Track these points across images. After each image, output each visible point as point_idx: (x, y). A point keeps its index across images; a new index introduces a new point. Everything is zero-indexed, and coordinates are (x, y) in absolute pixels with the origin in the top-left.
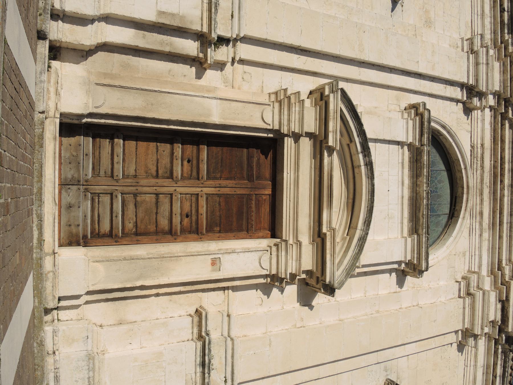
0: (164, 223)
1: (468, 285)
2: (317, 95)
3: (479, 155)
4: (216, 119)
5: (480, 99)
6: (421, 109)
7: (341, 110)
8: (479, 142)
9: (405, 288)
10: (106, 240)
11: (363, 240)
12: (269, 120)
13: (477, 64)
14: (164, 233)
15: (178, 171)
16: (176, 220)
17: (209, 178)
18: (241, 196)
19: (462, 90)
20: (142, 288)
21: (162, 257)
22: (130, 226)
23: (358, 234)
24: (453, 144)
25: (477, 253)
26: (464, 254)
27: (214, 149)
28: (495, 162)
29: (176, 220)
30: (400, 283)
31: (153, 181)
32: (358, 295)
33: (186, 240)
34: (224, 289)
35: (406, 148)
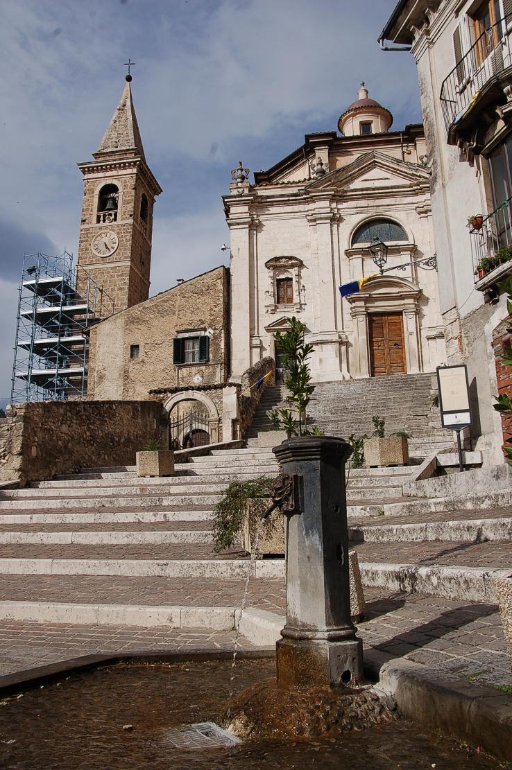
20: (419, 356)
34: (420, 330)
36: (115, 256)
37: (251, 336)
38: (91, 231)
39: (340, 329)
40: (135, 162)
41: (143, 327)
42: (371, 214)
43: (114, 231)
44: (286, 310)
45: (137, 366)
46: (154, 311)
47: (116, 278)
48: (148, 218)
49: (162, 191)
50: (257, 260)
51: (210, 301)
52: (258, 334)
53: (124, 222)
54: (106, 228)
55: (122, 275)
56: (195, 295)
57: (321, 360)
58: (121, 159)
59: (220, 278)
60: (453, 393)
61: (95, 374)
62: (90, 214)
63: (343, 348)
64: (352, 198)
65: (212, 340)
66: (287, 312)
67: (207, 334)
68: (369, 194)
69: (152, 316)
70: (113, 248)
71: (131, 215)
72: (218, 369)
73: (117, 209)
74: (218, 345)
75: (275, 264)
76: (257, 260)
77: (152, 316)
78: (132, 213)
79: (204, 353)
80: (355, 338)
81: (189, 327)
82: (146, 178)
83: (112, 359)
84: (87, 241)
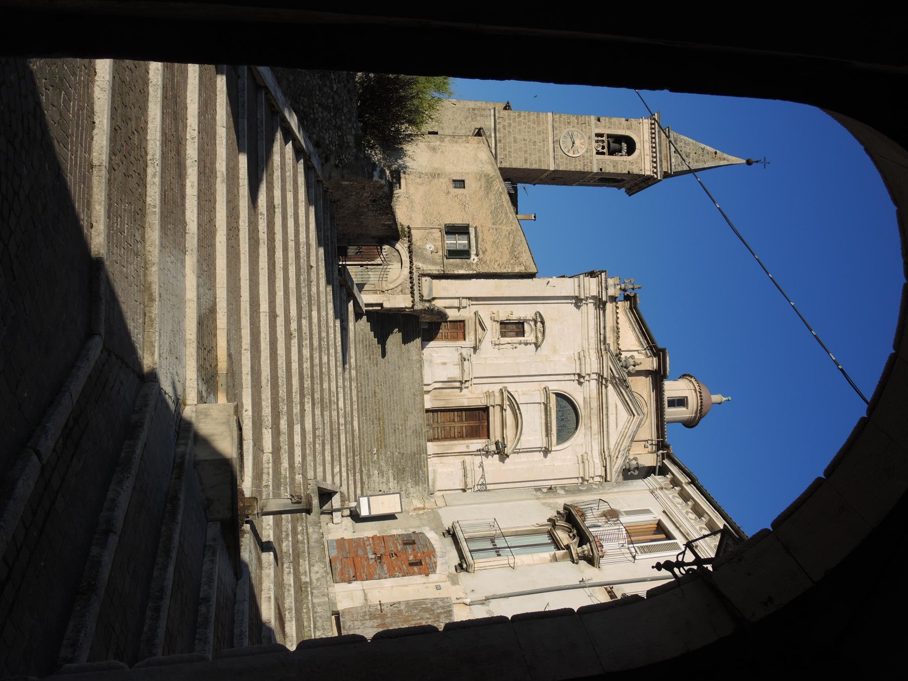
0: (452, 435)
1: (583, 459)
2: (501, 391)
3: (589, 401)
4: (466, 405)
5: (584, 379)
6: (547, 389)
7: (508, 396)
8: (588, 396)
9: (548, 458)
10: (437, 440)
11: (519, 439)
12: (483, 402)
13: (581, 364)
14: (453, 438)
15: (456, 420)
16: (456, 434)
17: (466, 421)
18: (477, 426)
19: (574, 375)
21: (452, 445)
22: (443, 436)
23: (518, 437)
24: (572, 399)
25: (590, 445)
26: (582, 445)
27: (467, 412)
28: (599, 403)
29: (456, 434)
30: (545, 456)
31: (449, 423)
32: (525, 460)
33: (459, 440)
34: (472, 455)
35: (542, 404)
36: (560, 153)
37: (469, 298)
38: (588, 127)
39: (475, 381)
40: (656, 173)
41: (482, 193)
42: (582, 412)
43: (587, 152)
44: (494, 331)
45: (444, 187)
46: (497, 204)
48: (600, 184)
49: (630, 195)
50: (543, 303)
51: (505, 260)
52: (472, 305)
53: (595, 162)
54: (590, 144)
55: (540, 161)
56: (511, 245)
57: (444, 364)
58: (661, 161)
59: (526, 270)
60: (383, 503)
61: (438, 143)
62: (605, 126)
63: (458, 384)
64: (600, 393)
65: (467, 262)
66: (493, 329)
67: (473, 257)
68: (602, 408)
69: (493, 201)
70: (569, 152)
71: (601, 169)
72: (438, 268)
73: (609, 155)
74: (462, 268)
75: (539, 320)
76: (543, 303)
77: (493, 201)
78: (603, 170)
79: (453, 253)
80: (466, 395)
81: (480, 239)
82: (641, 182)
83: (452, 161)
84: (578, 123)
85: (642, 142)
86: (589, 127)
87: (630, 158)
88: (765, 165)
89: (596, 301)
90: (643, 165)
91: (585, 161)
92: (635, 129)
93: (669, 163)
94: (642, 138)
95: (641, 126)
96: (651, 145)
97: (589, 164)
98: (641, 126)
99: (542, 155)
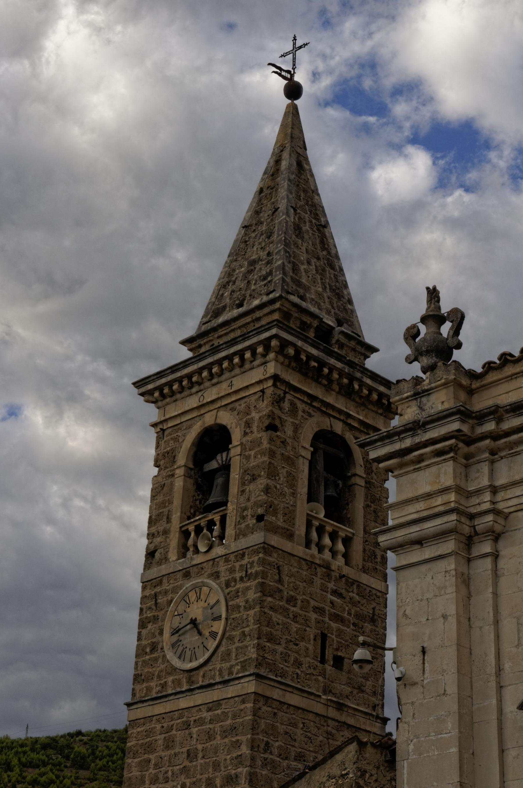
36: (217, 664)
40: (266, 343)
43: (216, 576)
47: (218, 741)
53: (243, 543)
55: (233, 728)
58: (234, 342)
70: (213, 635)
85: (202, 411)
86: (165, 581)
87: (236, 436)
88: (300, 47)
89: (480, 451)
90: (252, 391)
91: (238, 575)
92: (176, 440)
93: (258, 314)
94: (195, 414)
95: (170, 424)
96: (207, 384)
97: (246, 560)
98: (170, 424)
99: (217, 727)
